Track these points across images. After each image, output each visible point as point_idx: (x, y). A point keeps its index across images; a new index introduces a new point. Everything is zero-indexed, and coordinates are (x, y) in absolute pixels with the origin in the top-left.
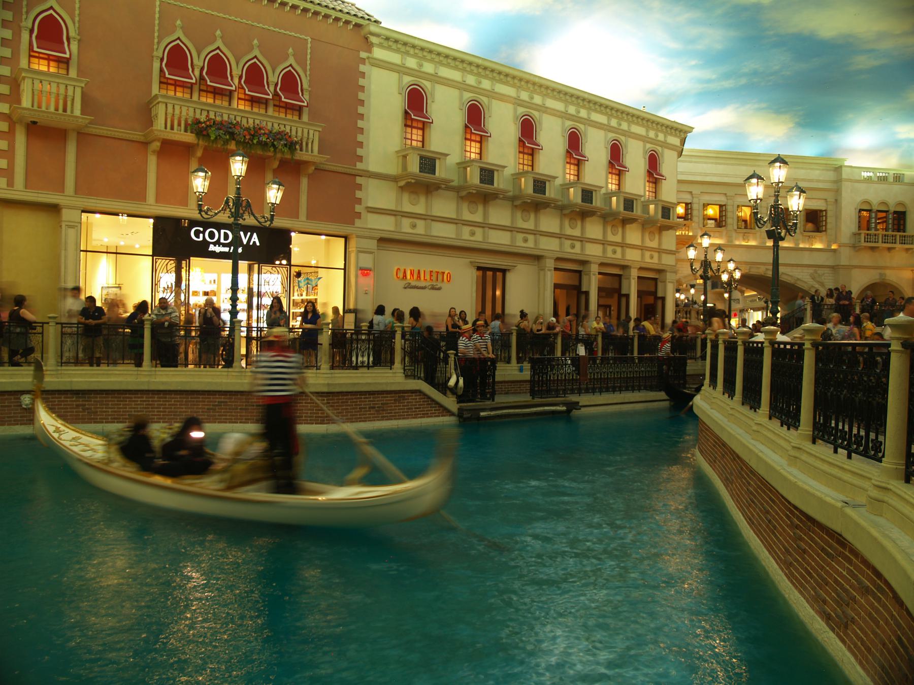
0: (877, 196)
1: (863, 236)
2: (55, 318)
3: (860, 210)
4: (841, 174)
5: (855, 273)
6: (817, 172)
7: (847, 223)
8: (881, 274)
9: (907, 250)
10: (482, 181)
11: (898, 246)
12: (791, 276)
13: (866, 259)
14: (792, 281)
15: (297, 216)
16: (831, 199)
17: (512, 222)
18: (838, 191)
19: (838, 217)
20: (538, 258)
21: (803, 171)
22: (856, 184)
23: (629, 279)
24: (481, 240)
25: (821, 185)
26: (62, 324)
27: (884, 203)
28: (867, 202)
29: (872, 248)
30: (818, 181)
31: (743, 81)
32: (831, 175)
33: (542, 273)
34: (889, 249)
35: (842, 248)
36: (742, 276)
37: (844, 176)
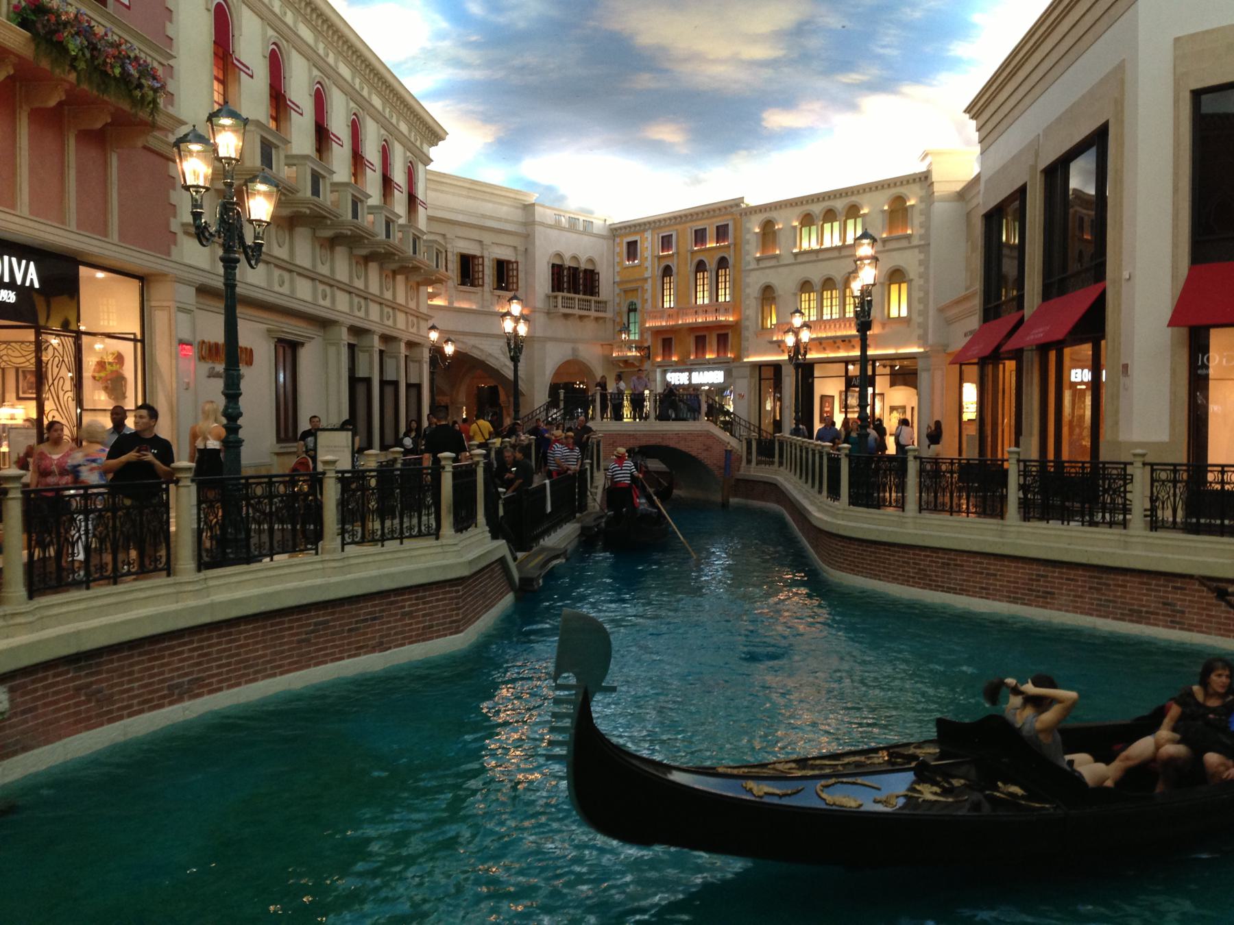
0: (578, 250)
1: (560, 299)
2: (1143, 455)
3: (553, 266)
4: (533, 215)
5: (550, 346)
6: (505, 209)
7: (542, 281)
8: (574, 350)
9: (597, 319)
10: (313, 194)
11: (593, 314)
12: (482, 350)
13: (560, 328)
14: (483, 358)
15: (104, 232)
16: (521, 248)
17: (314, 266)
18: (528, 237)
19: (530, 272)
20: (324, 324)
21: (490, 205)
22: (549, 231)
23: (397, 358)
24: (288, 293)
25: (508, 227)
26: (1152, 465)
27: (575, 258)
28: (559, 255)
29: (566, 316)
30: (506, 221)
31: (500, 74)
32: (518, 215)
33: (332, 350)
34: (581, 317)
35: (537, 315)
36: (456, 352)
37: (537, 218)
